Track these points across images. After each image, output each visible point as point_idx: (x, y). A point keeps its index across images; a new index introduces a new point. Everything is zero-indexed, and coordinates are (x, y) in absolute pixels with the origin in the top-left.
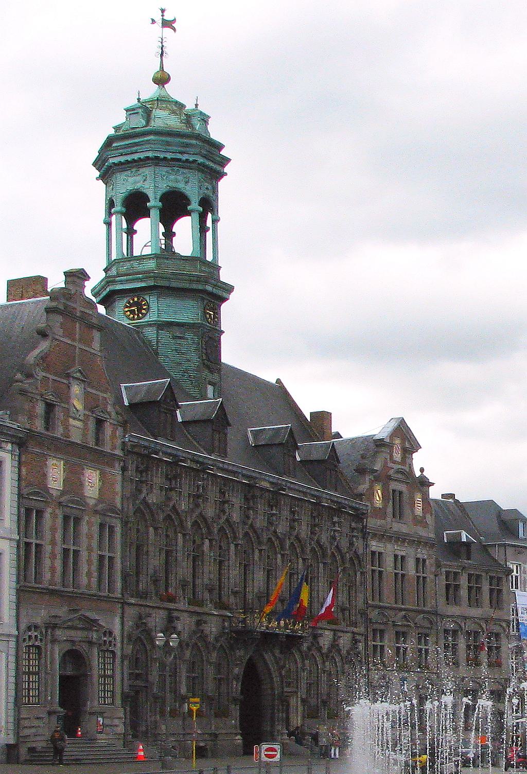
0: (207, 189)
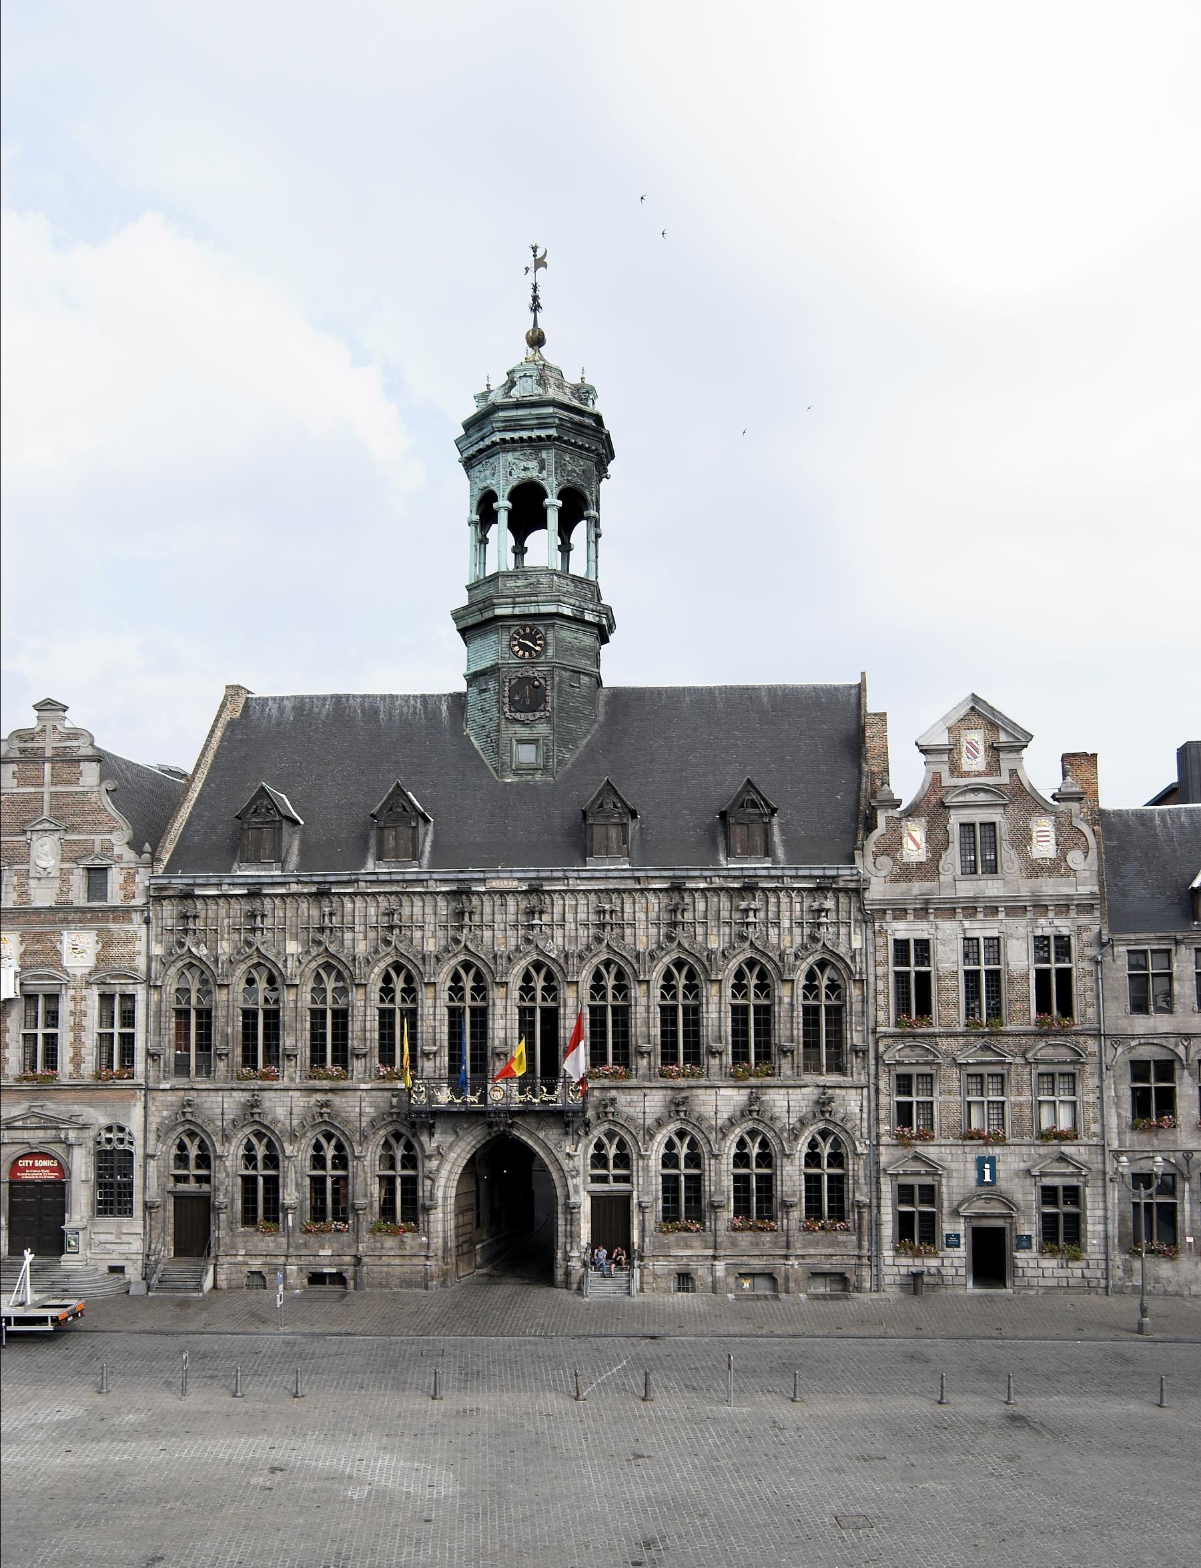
0: (525, 469)
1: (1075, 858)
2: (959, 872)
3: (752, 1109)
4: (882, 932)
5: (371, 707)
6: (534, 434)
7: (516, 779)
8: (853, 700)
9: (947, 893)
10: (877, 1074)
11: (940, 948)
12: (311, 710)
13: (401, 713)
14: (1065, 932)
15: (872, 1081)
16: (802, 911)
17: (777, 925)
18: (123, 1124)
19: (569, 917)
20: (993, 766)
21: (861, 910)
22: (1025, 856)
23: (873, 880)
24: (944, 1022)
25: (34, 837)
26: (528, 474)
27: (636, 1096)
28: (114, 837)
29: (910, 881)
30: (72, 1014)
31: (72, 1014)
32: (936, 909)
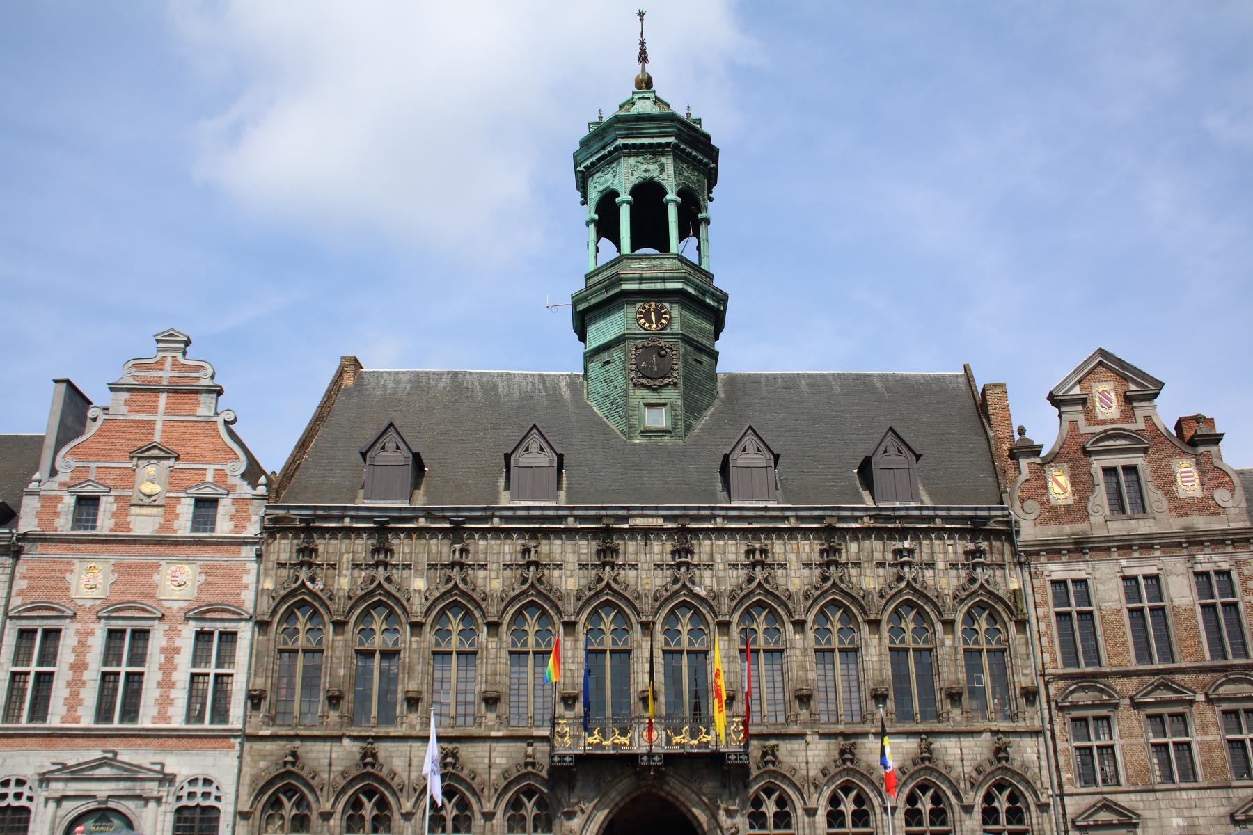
0: (646, 171)
1: (1221, 496)
2: (1108, 513)
3: (926, 758)
4: (1038, 574)
5: (488, 381)
6: (655, 141)
7: (645, 441)
8: (962, 384)
9: (1099, 533)
10: (1051, 718)
11: (1101, 587)
12: (428, 383)
13: (520, 389)
14: (1225, 566)
15: (1048, 726)
16: (955, 553)
17: (931, 566)
18: (211, 774)
19: (718, 558)
20: (1128, 415)
21: (1015, 553)
22: (1171, 495)
23: (1023, 524)
24: (1114, 662)
25: (140, 462)
26: (648, 175)
27: (797, 745)
28: (227, 468)
29: (1060, 523)
30: (163, 651)
31: (163, 651)
32: (1091, 549)
